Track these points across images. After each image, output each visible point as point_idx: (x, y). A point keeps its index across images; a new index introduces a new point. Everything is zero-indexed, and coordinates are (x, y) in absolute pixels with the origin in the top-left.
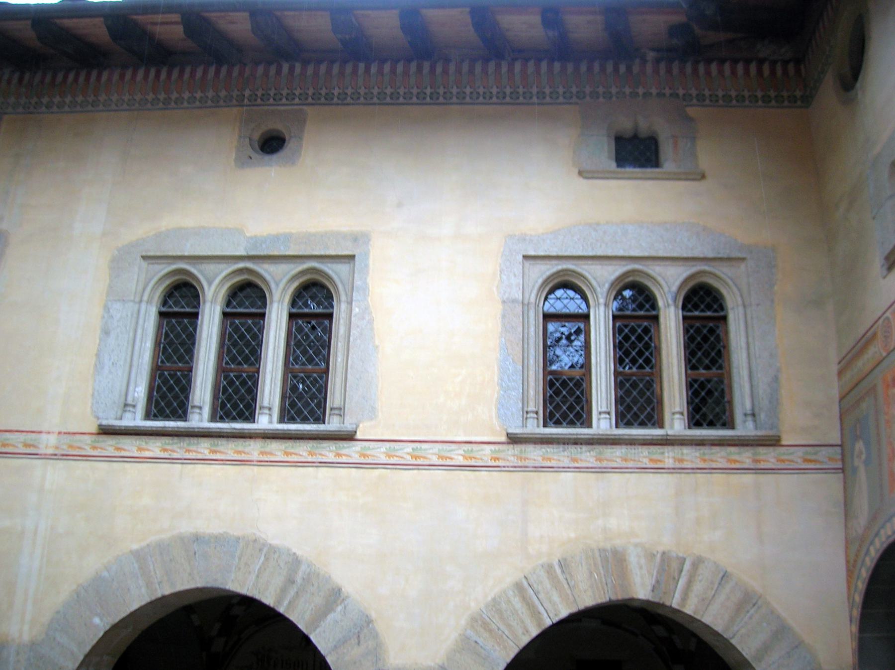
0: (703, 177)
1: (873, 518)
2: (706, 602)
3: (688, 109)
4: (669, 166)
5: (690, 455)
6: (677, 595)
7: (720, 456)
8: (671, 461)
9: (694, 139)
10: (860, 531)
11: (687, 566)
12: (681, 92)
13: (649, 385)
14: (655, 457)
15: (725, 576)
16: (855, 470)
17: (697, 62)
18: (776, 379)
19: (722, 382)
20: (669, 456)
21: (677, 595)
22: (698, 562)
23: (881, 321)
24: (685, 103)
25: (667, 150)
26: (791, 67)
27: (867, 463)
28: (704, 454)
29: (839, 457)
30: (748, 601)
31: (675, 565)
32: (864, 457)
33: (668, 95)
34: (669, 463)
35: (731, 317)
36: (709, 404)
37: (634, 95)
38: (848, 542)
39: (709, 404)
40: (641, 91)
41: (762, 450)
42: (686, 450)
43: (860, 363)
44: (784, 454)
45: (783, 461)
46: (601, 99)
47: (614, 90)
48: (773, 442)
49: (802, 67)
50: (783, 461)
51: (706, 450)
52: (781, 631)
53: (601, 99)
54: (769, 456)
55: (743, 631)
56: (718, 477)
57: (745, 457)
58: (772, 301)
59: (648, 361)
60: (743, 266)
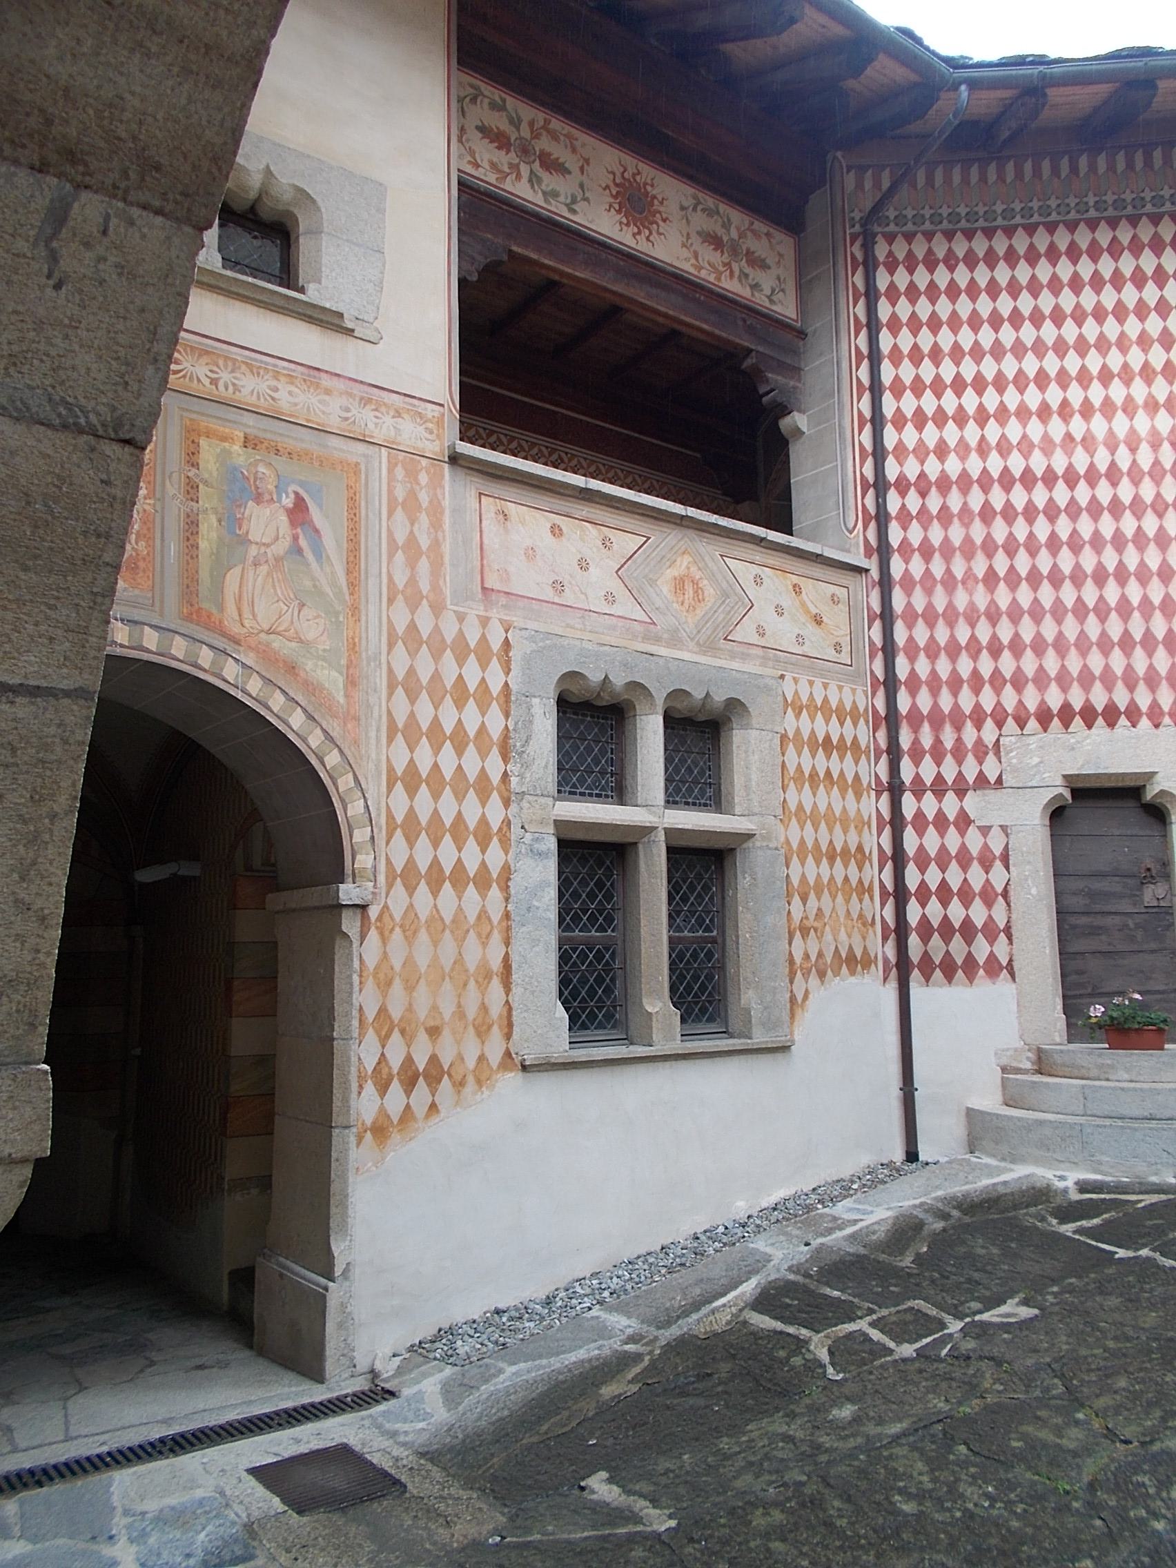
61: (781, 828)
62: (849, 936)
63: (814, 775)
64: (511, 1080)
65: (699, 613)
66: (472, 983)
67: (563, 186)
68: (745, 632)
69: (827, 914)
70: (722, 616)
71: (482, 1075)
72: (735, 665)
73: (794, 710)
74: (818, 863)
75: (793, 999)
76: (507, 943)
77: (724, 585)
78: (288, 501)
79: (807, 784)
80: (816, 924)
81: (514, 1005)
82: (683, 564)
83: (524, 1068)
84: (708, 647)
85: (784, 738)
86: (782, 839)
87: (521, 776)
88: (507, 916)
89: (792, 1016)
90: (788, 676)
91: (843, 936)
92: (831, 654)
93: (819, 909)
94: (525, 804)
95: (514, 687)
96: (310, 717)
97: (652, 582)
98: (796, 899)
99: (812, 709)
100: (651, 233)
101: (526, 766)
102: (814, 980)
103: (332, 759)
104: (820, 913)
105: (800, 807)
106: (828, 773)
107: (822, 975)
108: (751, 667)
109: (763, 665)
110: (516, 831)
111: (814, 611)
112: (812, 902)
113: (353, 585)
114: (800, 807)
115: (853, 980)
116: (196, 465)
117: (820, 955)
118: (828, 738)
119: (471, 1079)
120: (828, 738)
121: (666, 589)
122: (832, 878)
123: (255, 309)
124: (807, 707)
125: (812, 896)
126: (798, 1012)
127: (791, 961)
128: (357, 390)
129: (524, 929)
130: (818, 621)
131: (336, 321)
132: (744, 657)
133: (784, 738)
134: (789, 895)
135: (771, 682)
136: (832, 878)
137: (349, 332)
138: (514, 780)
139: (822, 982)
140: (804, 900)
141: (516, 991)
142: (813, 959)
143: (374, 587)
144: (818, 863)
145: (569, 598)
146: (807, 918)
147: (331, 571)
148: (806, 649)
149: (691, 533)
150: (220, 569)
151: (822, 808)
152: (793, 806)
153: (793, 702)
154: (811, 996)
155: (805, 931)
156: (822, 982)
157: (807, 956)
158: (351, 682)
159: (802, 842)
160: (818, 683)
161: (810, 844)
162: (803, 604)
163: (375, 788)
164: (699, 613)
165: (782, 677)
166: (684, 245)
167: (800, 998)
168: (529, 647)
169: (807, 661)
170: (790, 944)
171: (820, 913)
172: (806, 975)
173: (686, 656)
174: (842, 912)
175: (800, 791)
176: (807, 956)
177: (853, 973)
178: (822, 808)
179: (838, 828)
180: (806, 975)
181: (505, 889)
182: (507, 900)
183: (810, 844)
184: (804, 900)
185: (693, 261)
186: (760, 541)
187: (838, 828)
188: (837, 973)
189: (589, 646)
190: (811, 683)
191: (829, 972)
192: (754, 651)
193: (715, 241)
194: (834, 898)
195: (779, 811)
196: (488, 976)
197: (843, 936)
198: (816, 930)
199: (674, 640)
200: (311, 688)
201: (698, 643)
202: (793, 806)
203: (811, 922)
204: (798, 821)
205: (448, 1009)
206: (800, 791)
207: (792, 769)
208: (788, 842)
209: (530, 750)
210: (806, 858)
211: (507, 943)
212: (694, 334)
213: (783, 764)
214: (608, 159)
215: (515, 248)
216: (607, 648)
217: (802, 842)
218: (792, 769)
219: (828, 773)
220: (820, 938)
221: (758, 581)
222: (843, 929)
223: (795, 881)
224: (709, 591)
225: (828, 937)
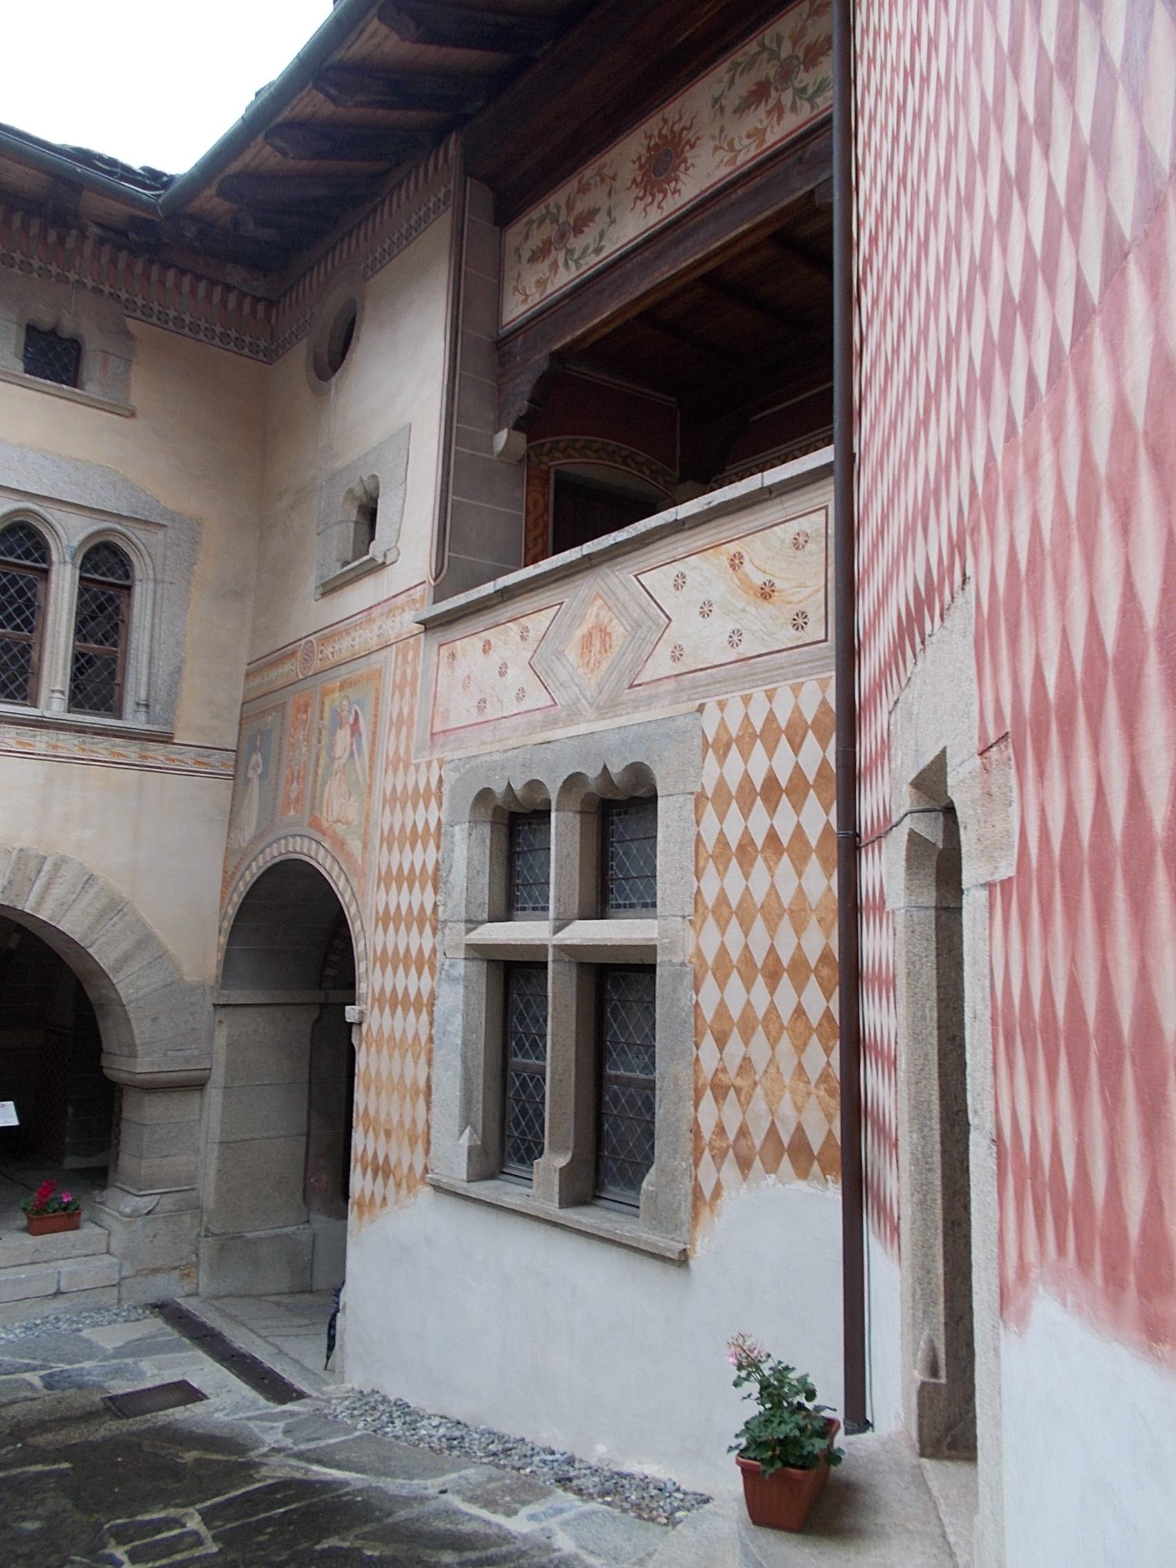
0: (133, 415)
1: (259, 836)
2: (65, 907)
3: (129, 320)
4: (92, 389)
5: (69, 743)
6: (32, 899)
7: (102, 747)
8: (43, 745)
9: (129, 362)
10: (244, 845)
11: (47, 867)
12: (124, 295)
13: (26, 650)
14: (26, 739)
15: (91, 879)
16: (248, 781)
17: (151, 262)
18: (179, 670)
19: (114, 661)
20: (41, 741)
21: (32, 899)
22: (61, 862)
23: (303, 642)
24: (126, 312)
25: (92, 367)
26: (261, 307)
27: (262, 777)
28: (84, 742)
29: (233, 763)
30: (114, 907)
31: (33, 865)
32: (259, 771)
33: (106, 293)
34: (40, 748)
35: (138, 589)
36: (96, 684)
37: (65, 280)
38: (228, 852)
39: (96, 684)
40: (73, 276)
41: (151, 745)
42: (62, 735)
43: (273, 674)
44: (175, 753)
45: (173, 760)
46: (16, 270)
47: (36, 263)
48: (165, 739)
49: (274, 311)
50: (173, 760)
51: (88, 738)
52: (147, 940)
53: (16, 270)
54: (158, 753)
55: (103, 939)
56: (95, 770)
57: (132, 751)
58: (189, 582)
59: (27, 622)
60: (161, 534)
61: (691, 933)
62: (799, 1109)
63: (746, 845)
64: (426, 1192)
65: (605, 665)
66: (408, 1099)
67: (589, 236)
68: (661, 665)
69: (760, 1066)
70: (630, 657)
71: (409, 1184)
72: (639, 717)
73: (716, 753)
74: (748, 984)
75: (697, 1191)
76: (429, 1064)
77: (637, 613)
78: (351, 720)
79: (734, 861)
80: (739, 1082)
81: (432, 1124)
82: (594, 613)
83: (437, 1188)
84: (609, 707)
85: (700, 799)
86: (691, 949)
87: (445, 905)
88: (431, 1039)
89: (695, 1216)
90: (711, 704)
91: (786, 1107)
92: (789, 636)
93: (746, 1059)
94: (447, 931)
95: (443, 820)
96: (347, 880)
97: (559, 654)
98: (709, 1042)
99: (747, 738)
100: (641, 199)
101: (448, 894)
102: (730, 1171)
103: (353, 909)
104: (746, 1065)
105: (722, 899)
106: (772, 837)
107: (744, 1165)
108: (657, 712)
109: (676, 701)
110: (439, 955)
111: (758, 579)
112: (735, 1047)
113: (371, 768)
114: (722, 899)
115: (801, 1185)
116: (322, 718)
117: (743, 1132)
118: (771, 780)
119: (404, 1182)
120: (771, 780)
121: (572, 655)
122: (772, 1009)
123: (349, 587)
124: (739, 740)
125: (735, 1038)
126: (705, 1212)
127: (696, 1131)
128: (386, 607)
129: (441, 1053)
130: (766, 593)
131: (371, 566)
132: (650, 701)
133: (700, 799)
134: (698, 1034)
135: (680, 722)
136: (772, 1009)
137: (383, 565)
138: (441, 909)
139: (745, 1177)
140: (721, 1041)
141: (434, 1110)
142: (732, 1135)
143: (380, 763)
144: (748, 984)
145: (490, 713)
146: (724, 1070)
147: (362, 763)
148: (746, 649)
149: (604, 570)
150: (324, 783)
151: (759, 895)
152: (710, 898)
153: (716, 740)
154: (725, 1194)
155: (720, 1091)
156: (745, 1177)
157: (720, 1130)
158: (365, 847)
159: (723, 951)
160: (759, 694)
161: (735, 954)
162: (745, 582)
163: (369, 929)
164: (605, 665)
165: (701, 709)
166: (717, 148)
167: (707, 1191)
168: (456, 775)
169: (743, 668)
170: (696, 1106)
171: (746, 1065)
172: (718, 1158)
173: (582, 729)
174: (787, 1065)
175: (722, 874)
176: (720, 1130)
177: (803, 1174)
178: (759, 895)
179: (786, 926)
180: (718, 1158)
181: (431, 1013)
182: (431, 1023)
183: (735, 954)
184: (721, 1041)
185: (728, 156)
186: (678, 527)
187: (786, 926)
188: (771, 1167)
189: (496, 757)
190: (747, 700)
191: (757, 1163)
192: (669, 685)
193: (760, 93)
194: (774, 1042)
195: (690, 909)
196: (417, 1095)
197: (786, 1107)
198: (738, 1091)
199: (573, 715)
200: (349, 856)
201: (598, 708)
202: (710, 898)
203: (731, 1077)
204: (717, 921)
205: (395, 1118)
206: (722, 874)
207: (710, 842)
208: (699, 953)
209: (451, 878)
210: (728, 976)
211: (429, 1064)
212: (753, 239)
213: (699, 840)
214: (630, 149)
215: (556, 347)
216: (510, 753)
217: (723, 951)
218: (710, 842)
219: (772, 837)
220: (744, 1105)
221: (680, 582)
222: (787, 1095)
223: (708, 1013)
224: (618, 631)
225: (759, 1104)
